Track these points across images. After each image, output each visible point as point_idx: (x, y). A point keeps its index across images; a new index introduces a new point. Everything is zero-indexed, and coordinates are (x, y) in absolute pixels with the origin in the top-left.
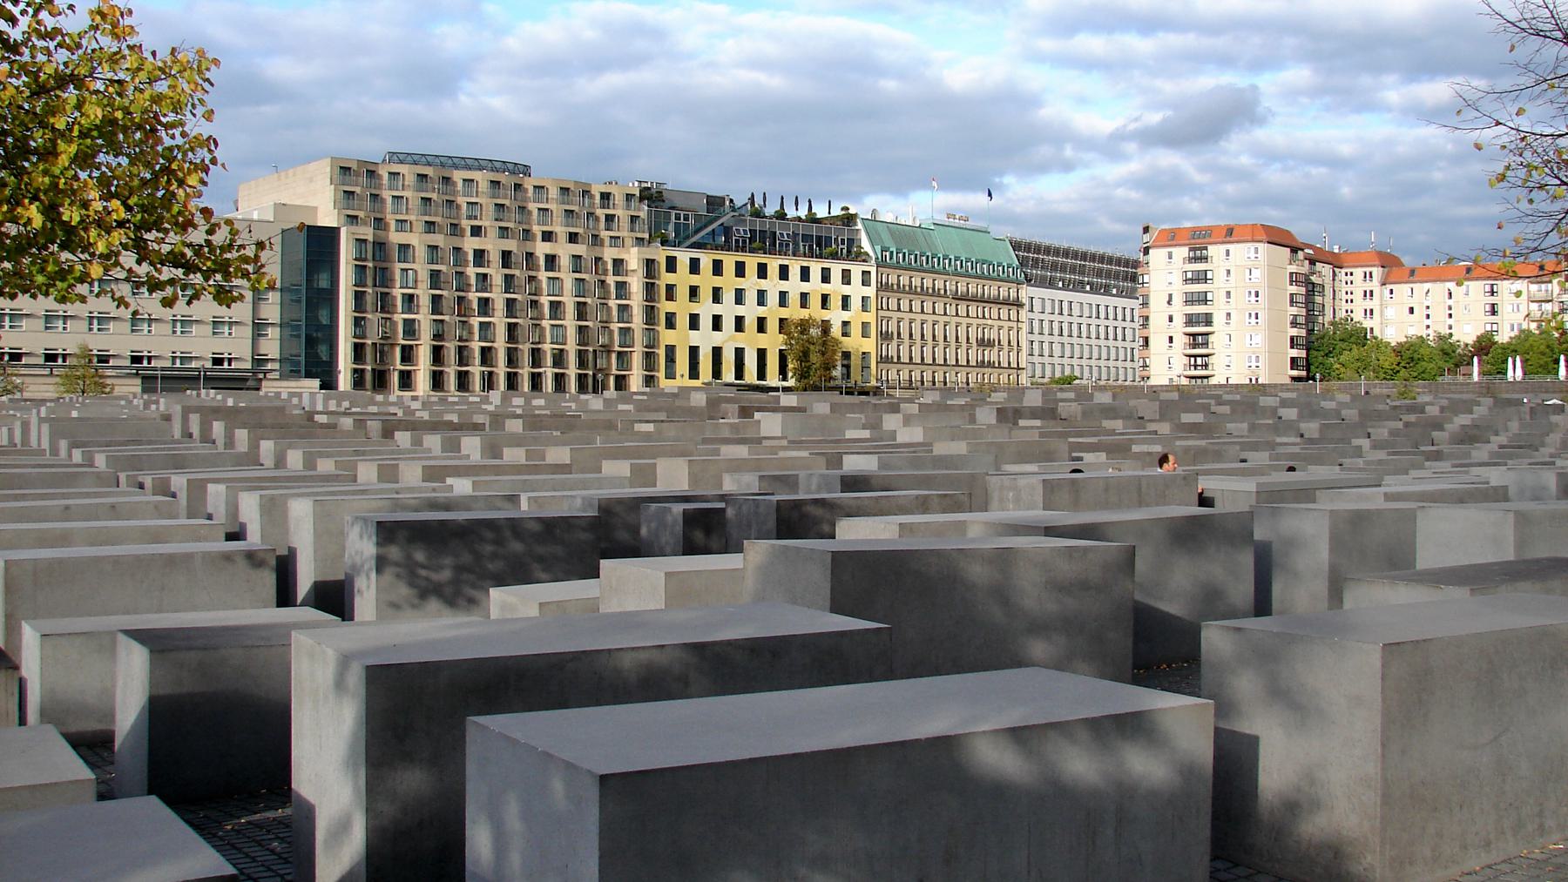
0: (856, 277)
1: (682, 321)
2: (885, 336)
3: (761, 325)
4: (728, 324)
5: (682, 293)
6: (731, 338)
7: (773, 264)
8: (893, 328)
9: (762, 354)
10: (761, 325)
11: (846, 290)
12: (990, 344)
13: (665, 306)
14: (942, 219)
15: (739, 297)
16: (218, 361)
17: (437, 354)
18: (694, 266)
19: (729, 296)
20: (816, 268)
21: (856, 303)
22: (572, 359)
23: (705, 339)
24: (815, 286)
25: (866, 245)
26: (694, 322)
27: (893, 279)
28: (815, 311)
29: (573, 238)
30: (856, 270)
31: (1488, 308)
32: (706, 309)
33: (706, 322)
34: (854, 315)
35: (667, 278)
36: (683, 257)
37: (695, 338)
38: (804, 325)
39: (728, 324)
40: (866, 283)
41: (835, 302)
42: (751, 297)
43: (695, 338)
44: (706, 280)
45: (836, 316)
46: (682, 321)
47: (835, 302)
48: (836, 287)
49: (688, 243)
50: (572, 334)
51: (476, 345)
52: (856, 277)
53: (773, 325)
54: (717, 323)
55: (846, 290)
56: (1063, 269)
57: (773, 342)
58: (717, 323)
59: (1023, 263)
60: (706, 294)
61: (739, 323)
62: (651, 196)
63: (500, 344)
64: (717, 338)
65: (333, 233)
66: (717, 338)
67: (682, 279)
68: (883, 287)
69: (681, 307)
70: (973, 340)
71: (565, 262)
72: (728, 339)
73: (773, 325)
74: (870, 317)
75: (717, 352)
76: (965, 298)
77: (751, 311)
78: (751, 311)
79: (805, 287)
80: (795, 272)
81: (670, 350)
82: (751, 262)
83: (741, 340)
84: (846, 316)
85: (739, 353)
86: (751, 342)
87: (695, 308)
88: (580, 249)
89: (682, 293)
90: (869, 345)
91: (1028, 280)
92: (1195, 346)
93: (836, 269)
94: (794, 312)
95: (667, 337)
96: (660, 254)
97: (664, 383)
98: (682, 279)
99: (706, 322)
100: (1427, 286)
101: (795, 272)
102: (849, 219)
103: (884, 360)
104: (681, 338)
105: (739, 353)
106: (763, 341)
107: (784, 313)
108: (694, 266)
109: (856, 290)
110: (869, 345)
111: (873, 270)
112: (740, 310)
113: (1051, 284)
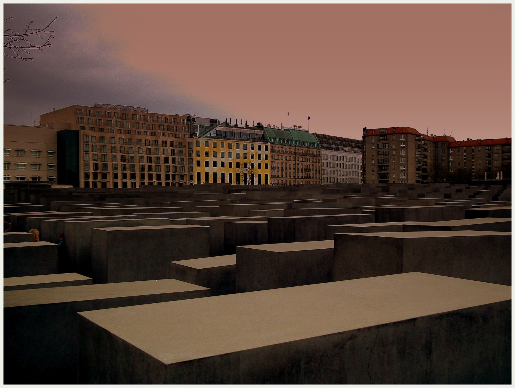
0: (263, 148)
1: (203, 164)
2: (273, 168)
3: (230, 165)
4: (219, 164)
6: (220, 170)
7: (234, 144)
8: (276, 166)
9: (230, 175)
10: (230, 165)
11: (260, 152)
12: (309, 170)
13: (196, 159)
14: (292, 127)
15: (223, 155)
16: (34, 179)
17: (116, 176)
19: (219, 155)
21: (263, 157)
22: (163, 177)
24: (248, 151)
25: (268, 136)
26: (207, 164)
27: (276, 149)
28: (248, 160)
30: (263, 145)
31: (487, 155)
32: (211, 160)
33: (211, 164)
34: (262, 161)
37: (207, 169)
38: (245, 165)
39: (219, 164)
40: (266, 149)
41: (256, 157)
42: (226, 155)
43: (207, 169)
45: (256, 162)
46: (203, 164)
47: (256, 157)
48: (256, 152)
49: (204, 136)
50: (163, 168)
51: (128, 173)
52: (263, 148)
53: (234, 165)
54: (215, 164)
55: (260, 152)
56: (335, 144)
57: (234, 170)
58: (215, 164)
59: (321, 142)
61: (223, 164)
64: (215, 170)
65: (77, 133)
66: (215, 170)
67: (202, 149)
68: (272, 151)
69: (202, 159)
70: (304, 169)
71: (160, 143)
72: (218, 170)
73: (234, 165)
74: (268, 162)
75: (215, 174)
76: (300, 154)
79: (245, 151)
80: (241, 146)
81: (199, 174)
83: (223, 170)
84: (260, 161)
85: (223, 174)
86: (226, 171)
87: (207, 159)
90: (268, 172)
91: (323, 148)
92: (382, 170)
94: (242, 161)
95: (197, 169)
99: (211, 164)
100: (465, 148)
101: (241, 146)
102: (260, 126)
103: (273, 176)
104: (202, 170)
105: (223, 174)
106: (231, 170)
107: (238, 161)
109: (263, 153)
111: (269, 145)
112: (223, 160)
113: (331, 149)
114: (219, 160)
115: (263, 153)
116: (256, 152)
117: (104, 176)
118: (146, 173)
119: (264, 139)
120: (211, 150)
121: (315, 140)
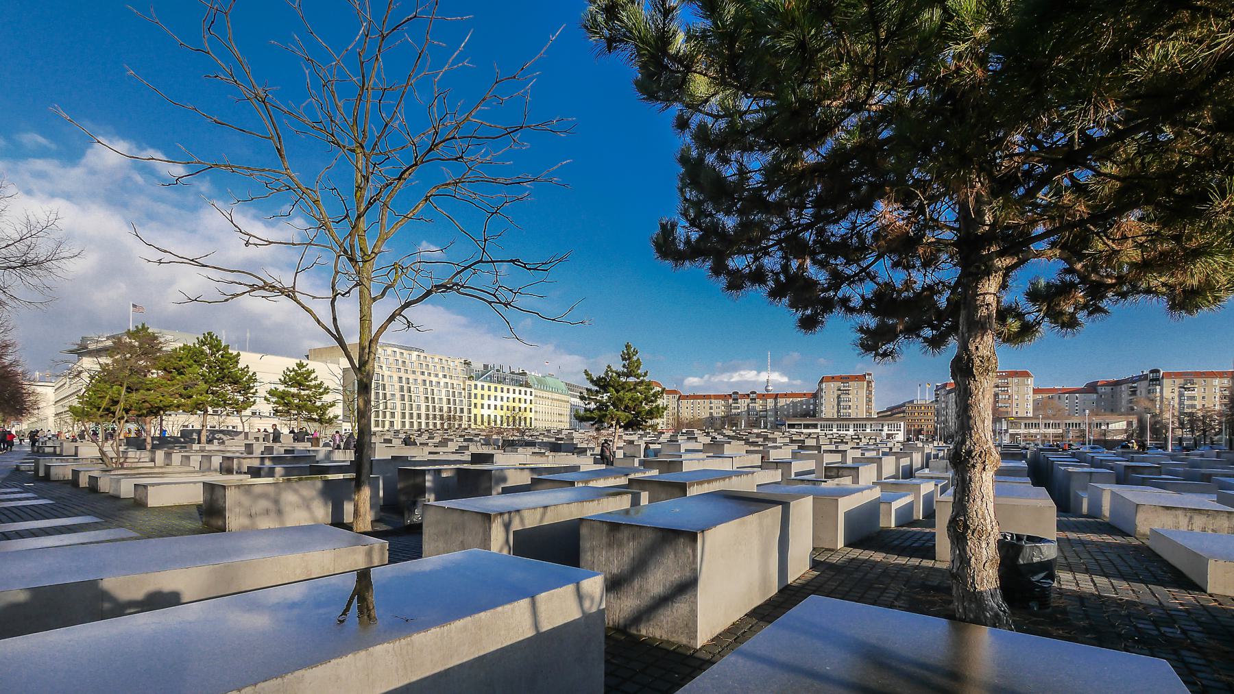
1: (479, 406)
5: (479, 396)
13: (473, 401)
17: (403, 415)
18: (483, 388)
20: (517, 389)
23: (486, 412)
28: (517, 404)
29: (445, 376)
30: (529, 390)
32: (486, 402)
33: (486, 406)
34: (528, 405)
35: (474, 391)
36: (479, 384)
37: (483, 412)
43: (483, 412)
44: (486, 393)
45: (523, 405)
46: (479, 406)
48: (523, 396)
60: (486, 397)
62: (467, 363)
63: (423, 412)
66: (489, 412)
69: (479, 401)
72: (492, 412)
77: (499, 403)
78: (499, 403)
82: (499, 387)
86: (499, 413)
88: (447, 380)
89: (479, 396)
93: (523, 389)
94: (511, 404)
95: (474, 411)
96: (473, 383)
97: (473, 426)
98: (479, 392)
99: (486, 406)
102: (524, 374)
108: (483, 388)
109: (528, 397)
110: (532, 415)
114: (492, 402)
115: (528, 397)
116: (523, 396)
117: (393, 415)
118: (431, 412)
119: (527, 385)
120: (486, 393)
121: (563, 386)
